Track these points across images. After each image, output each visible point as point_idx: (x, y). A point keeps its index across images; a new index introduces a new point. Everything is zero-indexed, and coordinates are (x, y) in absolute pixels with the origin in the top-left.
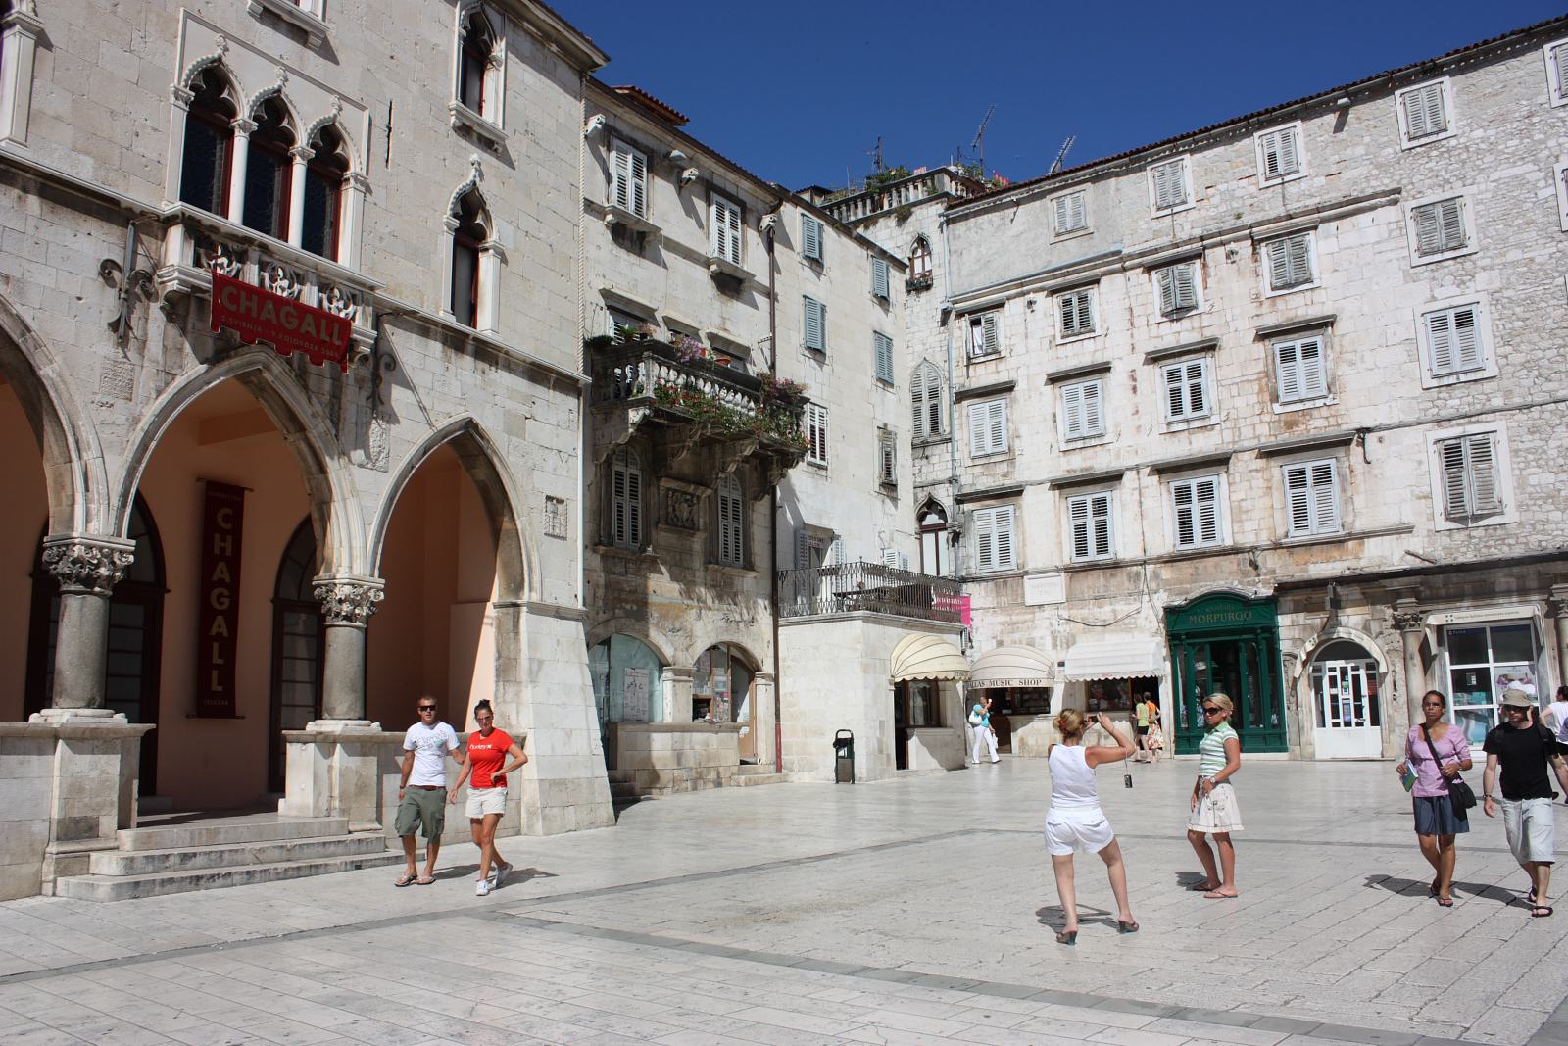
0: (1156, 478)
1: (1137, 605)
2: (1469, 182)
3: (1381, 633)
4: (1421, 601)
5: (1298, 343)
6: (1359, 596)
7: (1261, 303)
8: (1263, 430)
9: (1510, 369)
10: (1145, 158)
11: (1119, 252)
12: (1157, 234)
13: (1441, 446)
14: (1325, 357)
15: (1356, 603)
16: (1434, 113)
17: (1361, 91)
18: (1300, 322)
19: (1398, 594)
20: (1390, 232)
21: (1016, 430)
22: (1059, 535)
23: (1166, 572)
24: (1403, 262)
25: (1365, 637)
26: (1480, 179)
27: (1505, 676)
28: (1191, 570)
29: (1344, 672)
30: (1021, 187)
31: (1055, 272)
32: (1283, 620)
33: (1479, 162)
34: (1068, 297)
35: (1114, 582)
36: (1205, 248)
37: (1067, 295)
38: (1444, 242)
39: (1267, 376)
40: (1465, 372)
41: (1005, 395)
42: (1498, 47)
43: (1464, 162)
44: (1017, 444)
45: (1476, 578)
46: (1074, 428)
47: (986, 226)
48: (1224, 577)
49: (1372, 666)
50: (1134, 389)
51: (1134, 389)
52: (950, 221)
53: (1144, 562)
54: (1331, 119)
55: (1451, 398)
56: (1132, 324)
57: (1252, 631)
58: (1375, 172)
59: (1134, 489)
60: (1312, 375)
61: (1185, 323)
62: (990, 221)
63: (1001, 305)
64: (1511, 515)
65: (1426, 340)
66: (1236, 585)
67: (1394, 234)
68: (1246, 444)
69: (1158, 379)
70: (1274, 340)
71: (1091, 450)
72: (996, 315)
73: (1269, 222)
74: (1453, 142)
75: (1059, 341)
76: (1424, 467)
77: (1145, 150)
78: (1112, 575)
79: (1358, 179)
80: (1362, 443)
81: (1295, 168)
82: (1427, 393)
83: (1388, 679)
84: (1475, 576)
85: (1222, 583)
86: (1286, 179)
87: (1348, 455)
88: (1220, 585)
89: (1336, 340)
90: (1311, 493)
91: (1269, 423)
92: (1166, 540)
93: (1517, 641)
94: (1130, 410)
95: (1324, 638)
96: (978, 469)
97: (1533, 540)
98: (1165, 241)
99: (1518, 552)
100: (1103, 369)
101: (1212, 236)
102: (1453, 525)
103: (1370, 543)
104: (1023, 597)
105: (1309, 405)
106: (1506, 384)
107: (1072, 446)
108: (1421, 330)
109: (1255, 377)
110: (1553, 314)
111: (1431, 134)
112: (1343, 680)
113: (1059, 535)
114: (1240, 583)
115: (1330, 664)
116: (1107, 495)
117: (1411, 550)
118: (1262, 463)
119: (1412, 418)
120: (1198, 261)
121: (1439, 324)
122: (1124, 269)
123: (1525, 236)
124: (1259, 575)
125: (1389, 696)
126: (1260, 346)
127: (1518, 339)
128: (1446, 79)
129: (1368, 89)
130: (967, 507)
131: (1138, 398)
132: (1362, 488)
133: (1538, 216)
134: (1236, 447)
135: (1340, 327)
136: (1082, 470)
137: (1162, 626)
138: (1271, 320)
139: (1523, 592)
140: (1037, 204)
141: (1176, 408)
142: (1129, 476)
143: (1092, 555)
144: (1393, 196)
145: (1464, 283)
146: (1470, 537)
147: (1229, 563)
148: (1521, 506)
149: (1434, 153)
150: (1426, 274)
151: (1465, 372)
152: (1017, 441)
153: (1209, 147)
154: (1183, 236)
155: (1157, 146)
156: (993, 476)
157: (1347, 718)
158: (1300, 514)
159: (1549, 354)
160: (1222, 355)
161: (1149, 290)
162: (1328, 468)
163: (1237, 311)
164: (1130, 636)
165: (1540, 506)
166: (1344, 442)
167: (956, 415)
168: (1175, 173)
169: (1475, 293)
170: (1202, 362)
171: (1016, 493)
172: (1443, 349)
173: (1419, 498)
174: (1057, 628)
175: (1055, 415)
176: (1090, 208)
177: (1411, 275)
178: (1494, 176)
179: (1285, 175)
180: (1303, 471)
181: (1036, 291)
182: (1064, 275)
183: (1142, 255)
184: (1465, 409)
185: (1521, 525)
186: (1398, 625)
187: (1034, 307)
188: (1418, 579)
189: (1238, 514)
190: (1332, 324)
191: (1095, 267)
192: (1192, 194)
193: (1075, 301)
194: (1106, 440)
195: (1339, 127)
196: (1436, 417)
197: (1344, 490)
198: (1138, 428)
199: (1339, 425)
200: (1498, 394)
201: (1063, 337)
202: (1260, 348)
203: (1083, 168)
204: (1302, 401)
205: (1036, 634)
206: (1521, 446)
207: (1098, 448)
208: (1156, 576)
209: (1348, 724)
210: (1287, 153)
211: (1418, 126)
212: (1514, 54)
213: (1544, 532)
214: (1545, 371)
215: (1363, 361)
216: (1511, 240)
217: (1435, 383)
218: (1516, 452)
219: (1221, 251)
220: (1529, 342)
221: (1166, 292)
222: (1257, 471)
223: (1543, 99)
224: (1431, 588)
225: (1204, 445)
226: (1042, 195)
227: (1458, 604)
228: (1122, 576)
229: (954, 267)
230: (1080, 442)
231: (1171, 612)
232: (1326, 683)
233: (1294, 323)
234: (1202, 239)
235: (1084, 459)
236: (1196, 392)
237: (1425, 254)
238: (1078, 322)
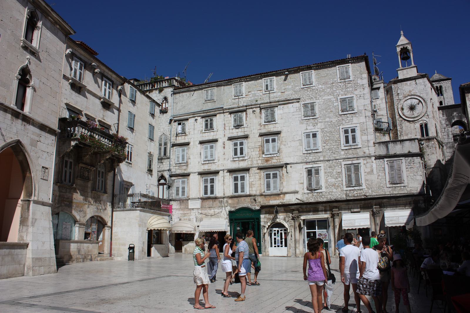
0: (229, 174)
1: (221, 210)
2: (318, 99)
3: (288, 221)
4: (299, 212)
5: (270, 138)
6: (283, 210)
7: (261, 126)
8: (260, 162)
9: (325, 150)
10: (232, 82)
11: (223, 108)
12: (234, 104)
13: (307, 169)
14: (278, 142)
15: (282, 212)
16: (310, 79)
17: (291, 71)
18: (271, 132)
19: (294, 210)
20: (297, 110)
21: (189, 157)
22: (200, 188)
23: (230, 201)
24: (300, 118)
25: (284, 222)
26: (320, 98)
27: (320, 234)
28: (237, 201)
29: (278, 231)
30: (196, 86)
31: (204, 111)
32: (262, 216)
33: (320, 94)
34: (207, 119)
35: (215, 203)
36: (247, 109)
37: (207, 119)
38: (310, 114)
39: (261, 147)
40: (314, 150)
41: (187, 146)
42: (326, 65)
43: (316, 93)
44: (189, 161)
45: (314, 206)
46: (206, 157)
47: (185, 96)
48: (246, 203)
49: (286, 230)
50: (224, 147)
51: (224, 147)
52: (174, 93)
53: (224, 198)
54: (283, 77)
55: (310, 157)
56: (225, 129)
57: (253, 219)
58: (294, 93)
59: (222, 176)
60: (274, 147)
61: (240, 130)
62: (186, 95)
63: (187, 119)
64: (324, 190)
65: (304, 140)
66: (250, 206)
67: (298, 110)
68: (254, 165)
69: (231, 145)
70: (264, 137)
71: (210, 164)
72: (186, 122)
73: (265, 103)
74: (314, 88)
75: (204, 132)
76: (302, 175)
77: (232, 79)
78: (214, 201)
79: (289, 94)
80: (286, 167)
81: (273, 89)
82: (304, 155)
83: (290, 234)
84: (314, 206)
85: (246, 205)
86: (270, 92)
87: (282, 170)
88: (245, 205)
89: (281, 138)
90: (272, 180)
91: (261, 160)
92: (230, 191)
93: (323, 224)
94: (223, 153)
95: (273, 222)
96: (177, 167)
97: (329, 197)
98: (236, 106)
99: (325, 200)
100: (216, 141)
101: (249, 106)
102: (309, 192)
103: (287, 195)
104: (188, 206)
105: (272, 156)
106: (324, 154)
107: (205, 162)
108: (303, 137)
109: (258, 147)
110: (336, 136)
111: (309, 85)
112: (278, 234)
113: (200, 188)
114: (250, 205)
115: (274, 229)
116: (214, 177)
117: (298, 198)
118: (258, 171)
119: (300, 161)
120: (245, 112)
121: (308, 136)
122: (224, 113)
123: (330, 115)
124: (256, 203)
125: (290, 239)
126: (260, 138)
127: (327, 142)
128: (313, 71)
129: (293, 70)
130: (173, 178)
131: (225, 150)
132: (285, 180)
133: (333, 110)
134: (252, 166)
135: (282, 135)
136: (207, 170)
137: (228, 216)
138: (264, 131)
139: (325, 211)
140: (200, 91)
141: (236, 154)
142: (221, 172)
143: (209, 195)
144: (298, 100)
145: (315, 126)
146: (313, 195)
147: (248, 199)
149: (309, 90)
150: (305, 122)
151: (314, 150)
152: (189, 160)
153: (250, 81)
154: (241, 105)
155: (236, 79)
156: (181, 170)
157: (278, 245)
158: (268, 186)
159: (335, 147)
160: (249, 140)
161: (230, 119)
162: (276, 174)
163: (254, 127)
164: (219, 219)
165: (331, 188)
166: (281, 167)
167: (171, 151)
168: (240, 87)
169: (318, 129)
170: (244, 141)
171: (188, 175)
172: (309, 143)
173: (300, 184)
174: (198, 216)
175: (201, 153)
176: (215, 94)
177: (302, 123)
178: (324, 98)
179: (270, 91)
180: (270, 174)
181: (198, 116)
182: (206, 113)
183: (229, 109)
184: (313, 160)
185: (326, 193)
186: (293, 219)
187: (197, 121)
188: (299, 206)
189: (251, 185)
190: (280, 133)
191: (216, 111)
192: (244, 93)
193: (209, 120)
194: (215, 161)
195: (285, 80)
196: (306, 162)
197: (280, 180)
198: (225, 159)
199: (280, 162)
200: (322, 157)
201: (205, 131)
202: (260, 139)
203: (214, 82)
204: (271, 154)
205: (191, 217)
206: (327, 171)
207: (213, 164)
208: (227, 202)
209: (278, 246)
210: (271, 85)
211: (305, 82)
212: (330, 67)
213: (331, 195)
214: (334, 151)
215: (287, 144)
216: (327, 115)
217: (306, 152)
219: (251, 110)
220: (330, 143)
221: (235, 120)
222: (257, 173)
223: (336, 80)
224: (302, 209)
225: (243, 165)
226: (202, 89)
227: (309, 214)
228: (217, 201)
229: (175, 107)
230: (209, 161)
231: (231, 213)
232: (273, 234)
233: (270, 132)
234: (246, 106)
235: (208, 167)
236: (242, 149)
237: (305, 117)
238: (209, 127)
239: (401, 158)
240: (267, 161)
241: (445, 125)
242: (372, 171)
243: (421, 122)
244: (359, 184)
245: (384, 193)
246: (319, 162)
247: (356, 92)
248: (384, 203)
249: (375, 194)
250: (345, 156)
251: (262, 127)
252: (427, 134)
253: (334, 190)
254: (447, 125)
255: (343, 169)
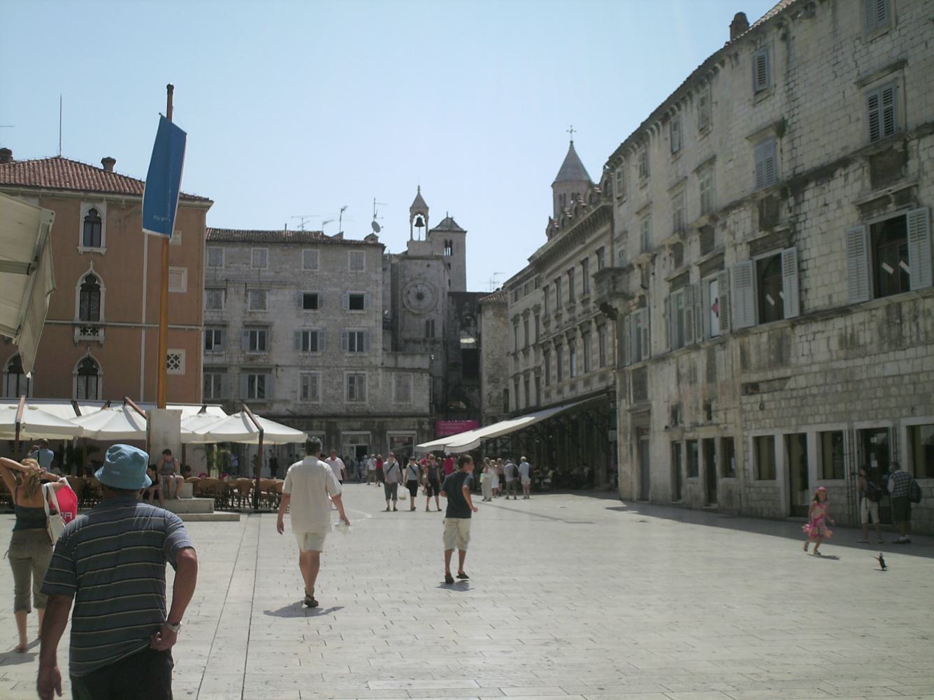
8: (241, 360)
58: (292, 276)
97: (326, 410)
99: (321, 413)
148: (324, 400)
166: (270, 370)
177: (299, 316)
184: (310, 365)
218: (324, 381)
239: (411, 374)
240: (251, 359)
241: (453, 318)
242: (378, 384)
243: (428, 318)
244: (362, 398)
245: (387, 411)
246: (317, 368)
247: (368, 289)
248: (387, 422)
249: (378, 411)
250: (347, 365)
251: (248, 315)
252: (433, 335)
253: (334, 403)
254: (456, 318)
255: (345, 380)
